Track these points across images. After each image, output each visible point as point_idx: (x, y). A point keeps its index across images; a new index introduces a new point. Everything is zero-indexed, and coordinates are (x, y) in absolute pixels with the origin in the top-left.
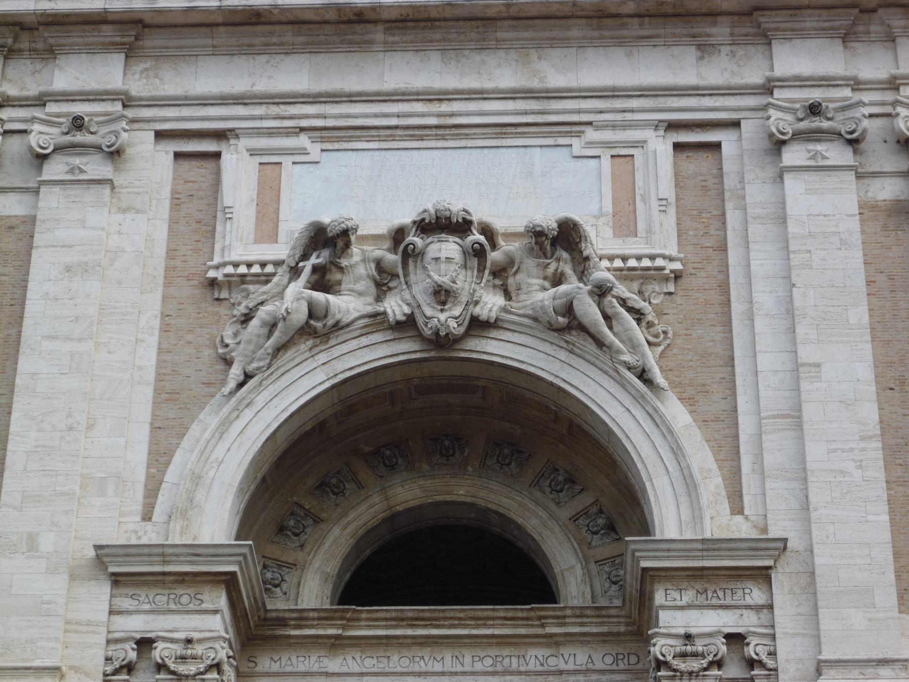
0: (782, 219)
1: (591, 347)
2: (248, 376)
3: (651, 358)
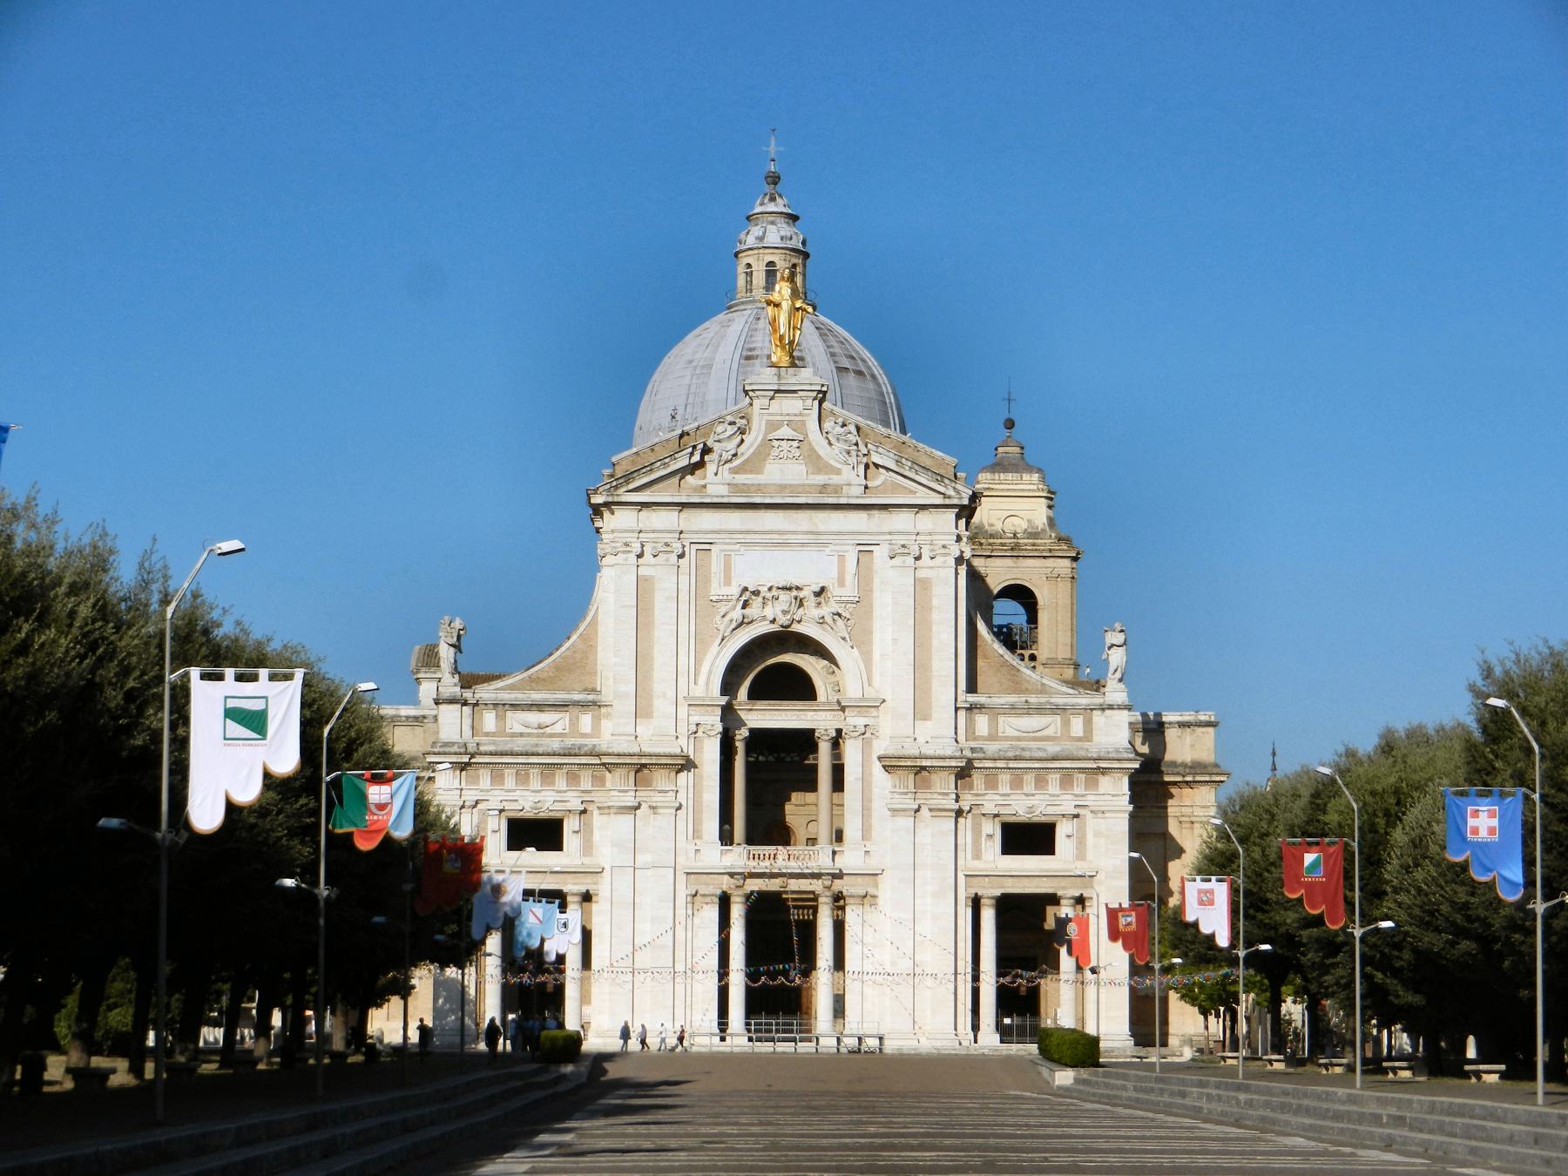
1: (830, 629)
3: (847, 637)
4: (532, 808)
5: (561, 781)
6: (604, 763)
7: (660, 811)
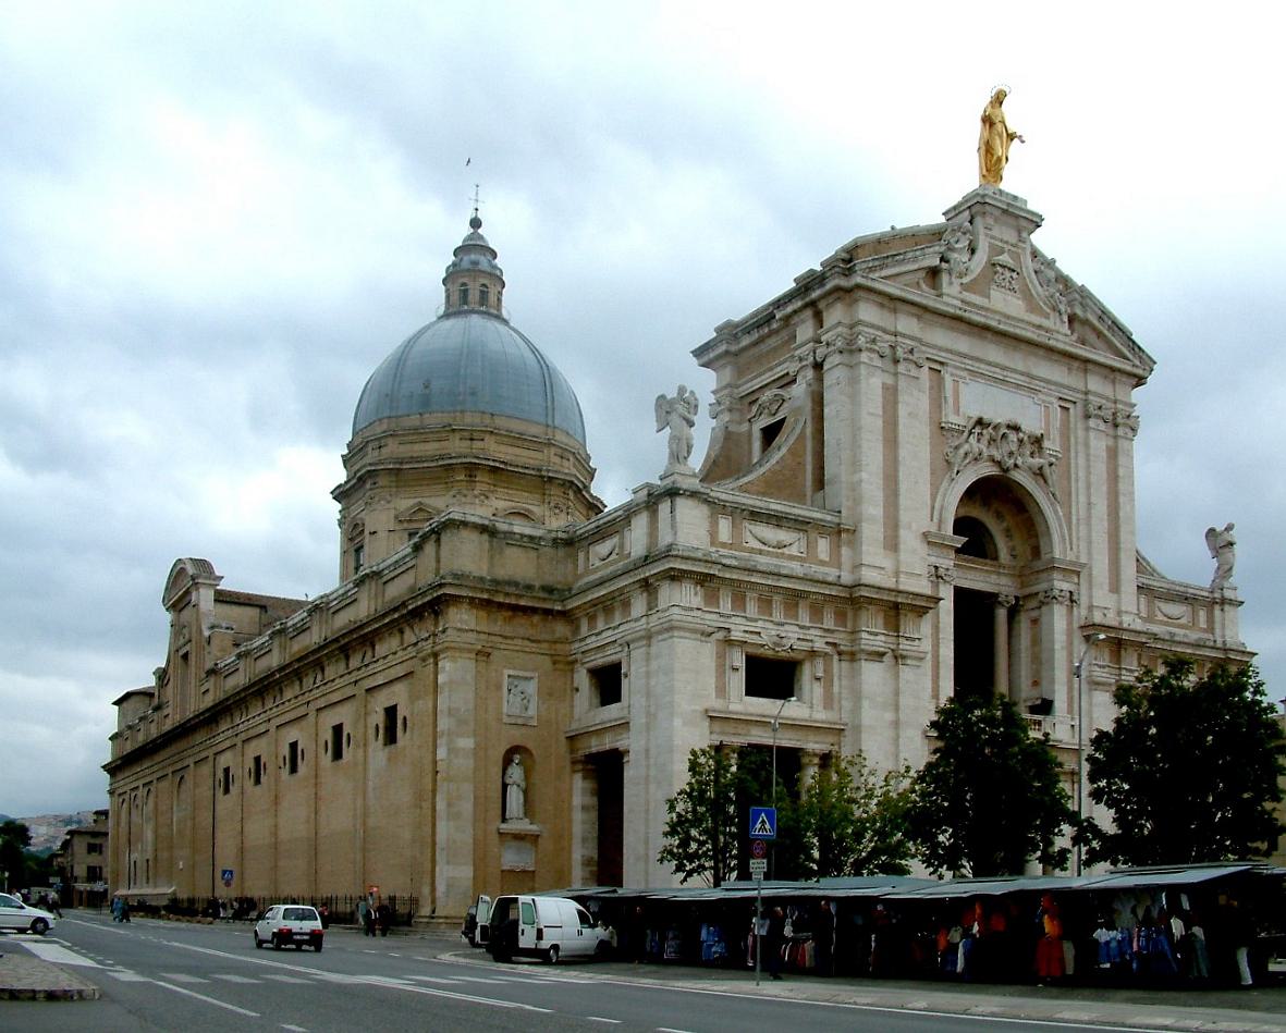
0: (1087, 445)
2: (958, 472)
4: (774, 643)
5: (804, 617)
6: (851, 601)
7: (909, 662)
